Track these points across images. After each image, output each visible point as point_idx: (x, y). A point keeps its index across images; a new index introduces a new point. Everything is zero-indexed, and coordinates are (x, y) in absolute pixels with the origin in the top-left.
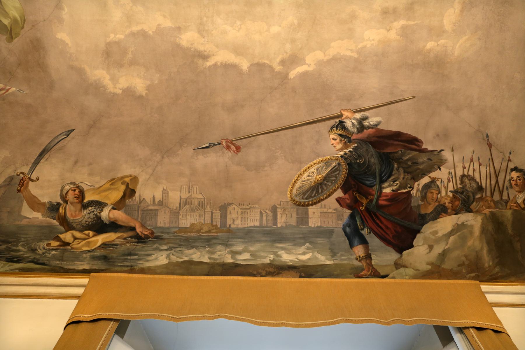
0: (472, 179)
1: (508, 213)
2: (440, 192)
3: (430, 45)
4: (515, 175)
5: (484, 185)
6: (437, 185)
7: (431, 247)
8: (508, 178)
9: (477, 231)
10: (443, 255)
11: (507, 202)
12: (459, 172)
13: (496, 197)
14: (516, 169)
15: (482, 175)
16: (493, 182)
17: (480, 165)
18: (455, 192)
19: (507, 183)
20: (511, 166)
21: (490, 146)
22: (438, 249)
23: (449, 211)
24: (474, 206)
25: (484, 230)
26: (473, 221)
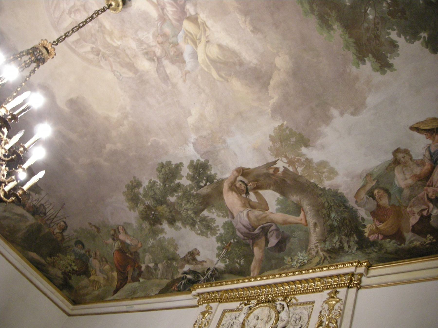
0: (45, 209)
1: (47, 230)
2: (28, 200)
3: (69, 159)
4: (62, 223)
5: (47, 214)
6: (29, 198)
7: (5, 211)
8: (59, 221)
9: (28, 224)
10: (6, 218)
11: (50, 227)
12: (42, 202)
13: (48, 222)
14: (65, 222)
15: (50, 212)
16: (52, 217)
17: (53, 208)
18: (34, 206)
19: (57, 222)
20: (64, 220)
21: (62, 207)
22: (7, 214)
23: (26, 208)
24: (37, 216)
25: (31, 226)
26: (31, 220)
